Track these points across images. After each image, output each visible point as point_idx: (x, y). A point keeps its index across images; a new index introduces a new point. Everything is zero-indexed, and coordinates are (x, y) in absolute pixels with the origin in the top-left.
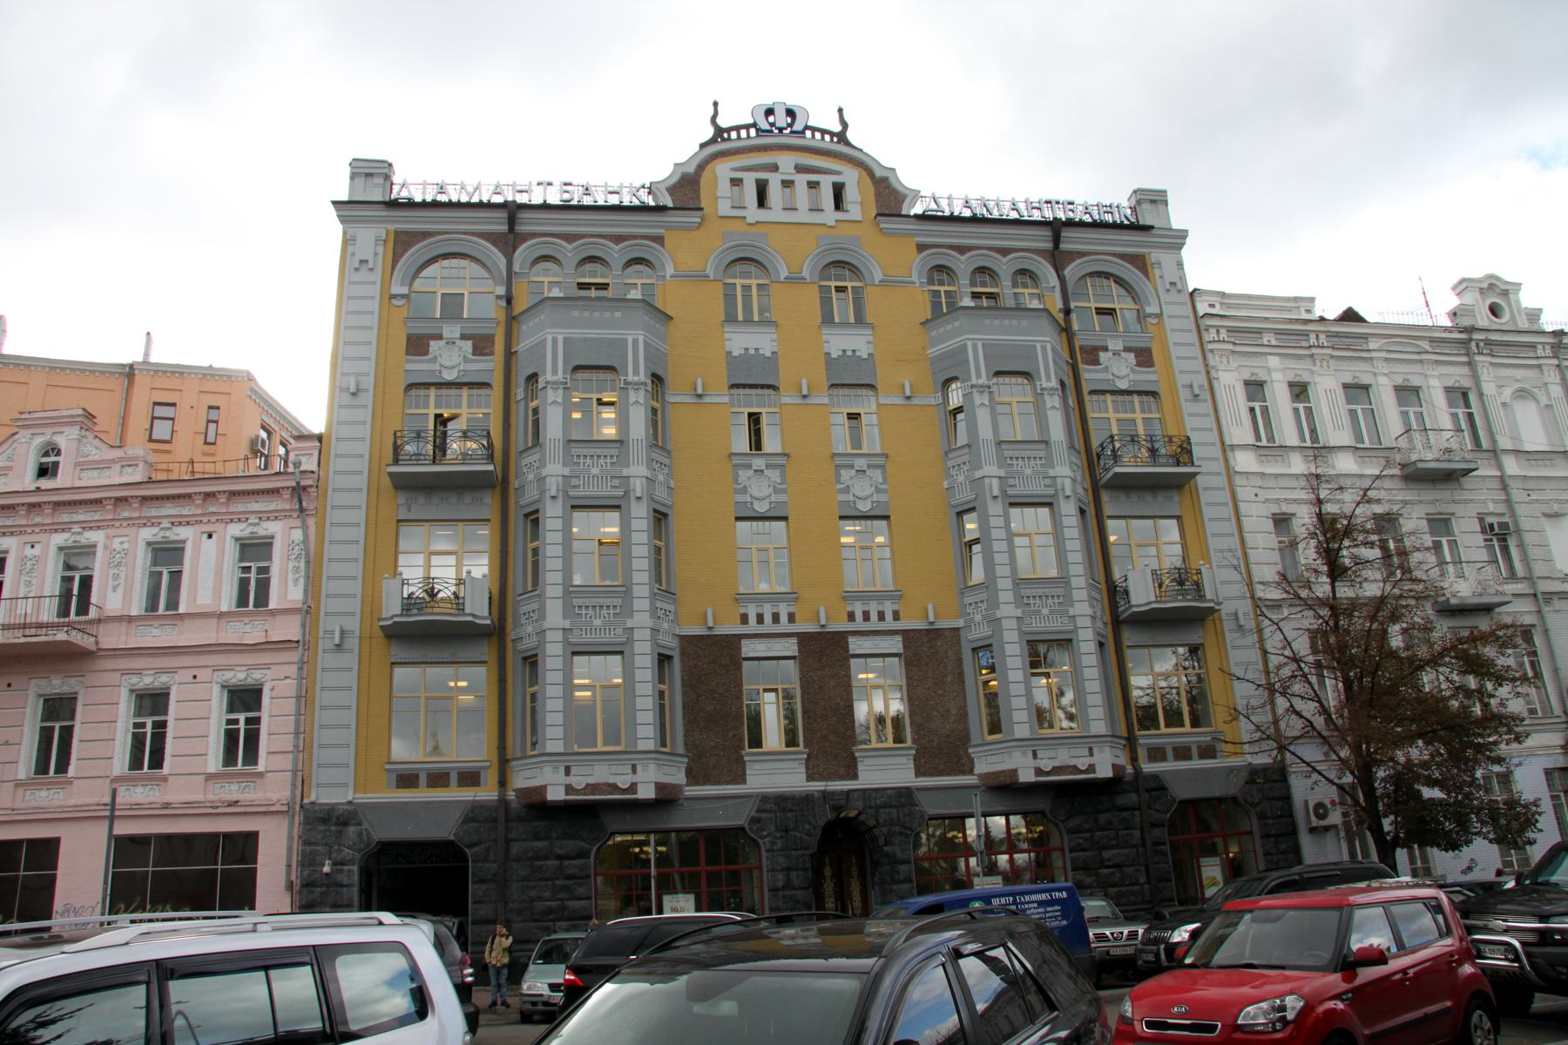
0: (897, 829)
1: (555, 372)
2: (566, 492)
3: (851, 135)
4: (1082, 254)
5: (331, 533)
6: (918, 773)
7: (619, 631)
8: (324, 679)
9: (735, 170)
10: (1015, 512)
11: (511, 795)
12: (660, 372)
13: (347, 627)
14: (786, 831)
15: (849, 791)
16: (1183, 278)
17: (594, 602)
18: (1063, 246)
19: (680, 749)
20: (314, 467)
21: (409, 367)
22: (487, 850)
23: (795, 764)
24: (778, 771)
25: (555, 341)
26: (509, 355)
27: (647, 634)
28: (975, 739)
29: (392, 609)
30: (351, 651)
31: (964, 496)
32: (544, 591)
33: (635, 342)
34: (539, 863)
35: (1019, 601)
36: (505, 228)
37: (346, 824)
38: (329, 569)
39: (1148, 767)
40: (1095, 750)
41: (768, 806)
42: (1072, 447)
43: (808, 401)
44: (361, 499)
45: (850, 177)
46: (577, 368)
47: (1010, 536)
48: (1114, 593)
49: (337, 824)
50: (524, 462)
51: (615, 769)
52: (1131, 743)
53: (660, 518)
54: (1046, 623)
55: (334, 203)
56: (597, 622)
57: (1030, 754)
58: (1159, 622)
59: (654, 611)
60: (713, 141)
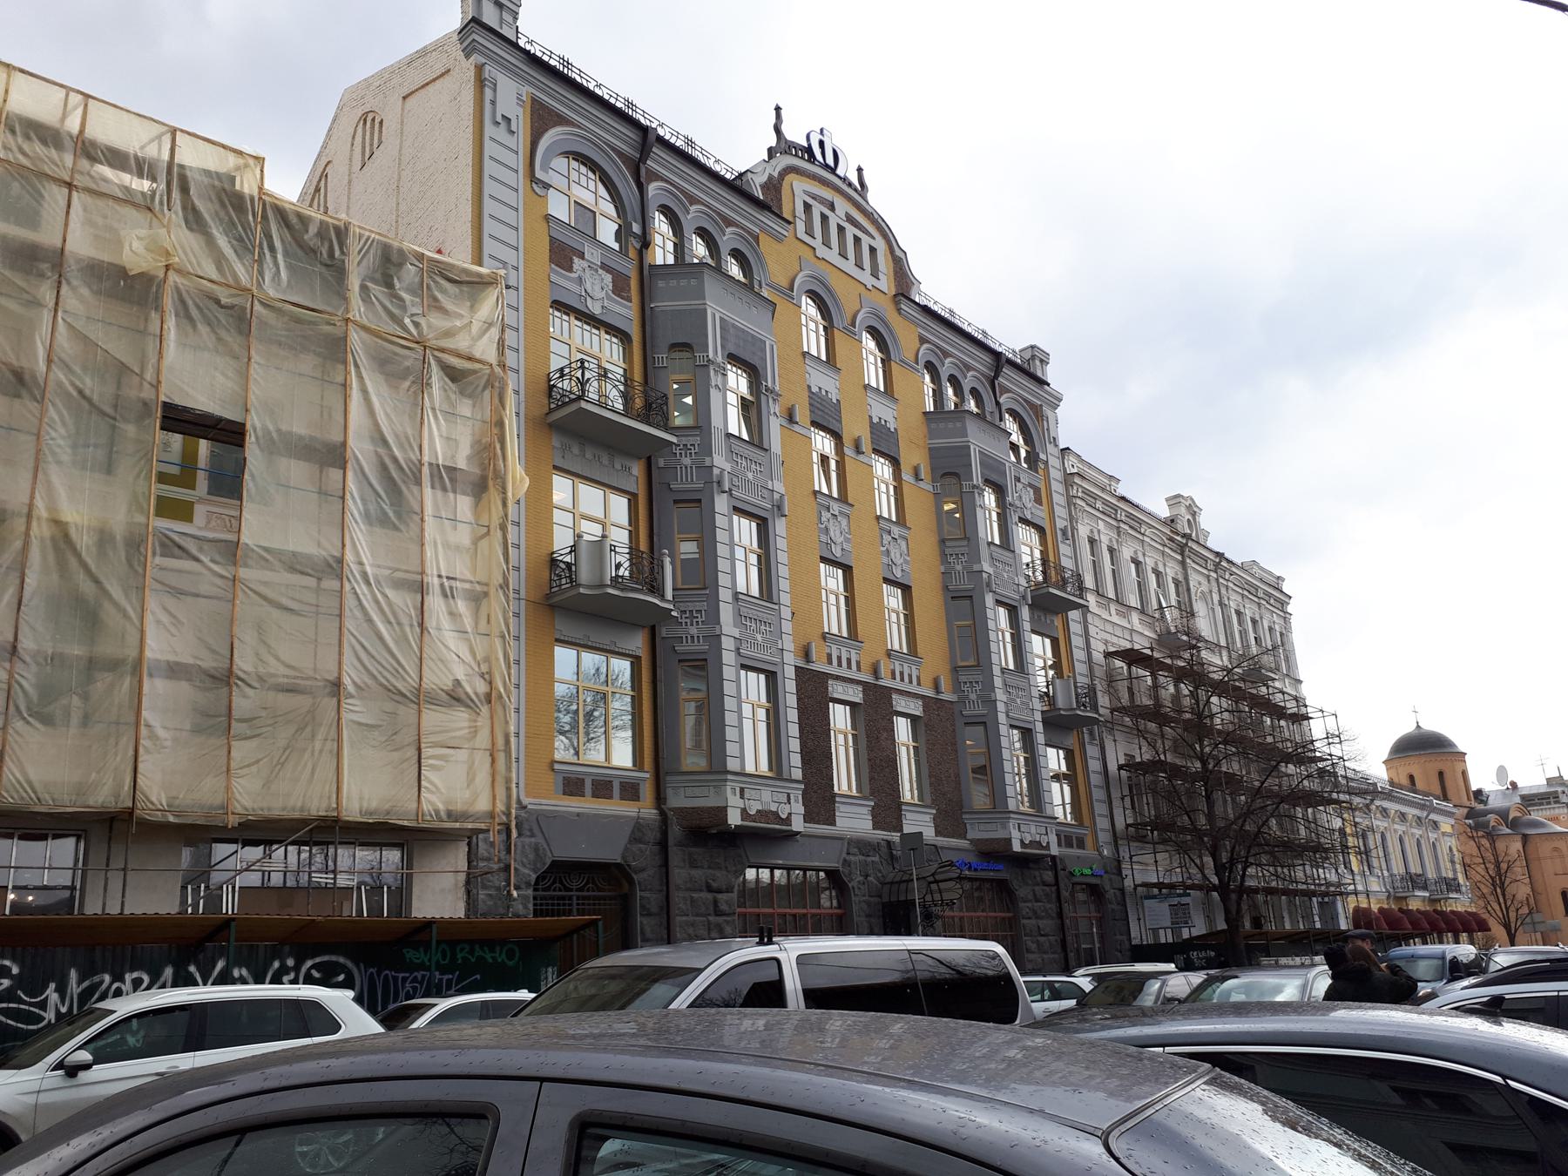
6: (938, 833)
24: (855, 821)
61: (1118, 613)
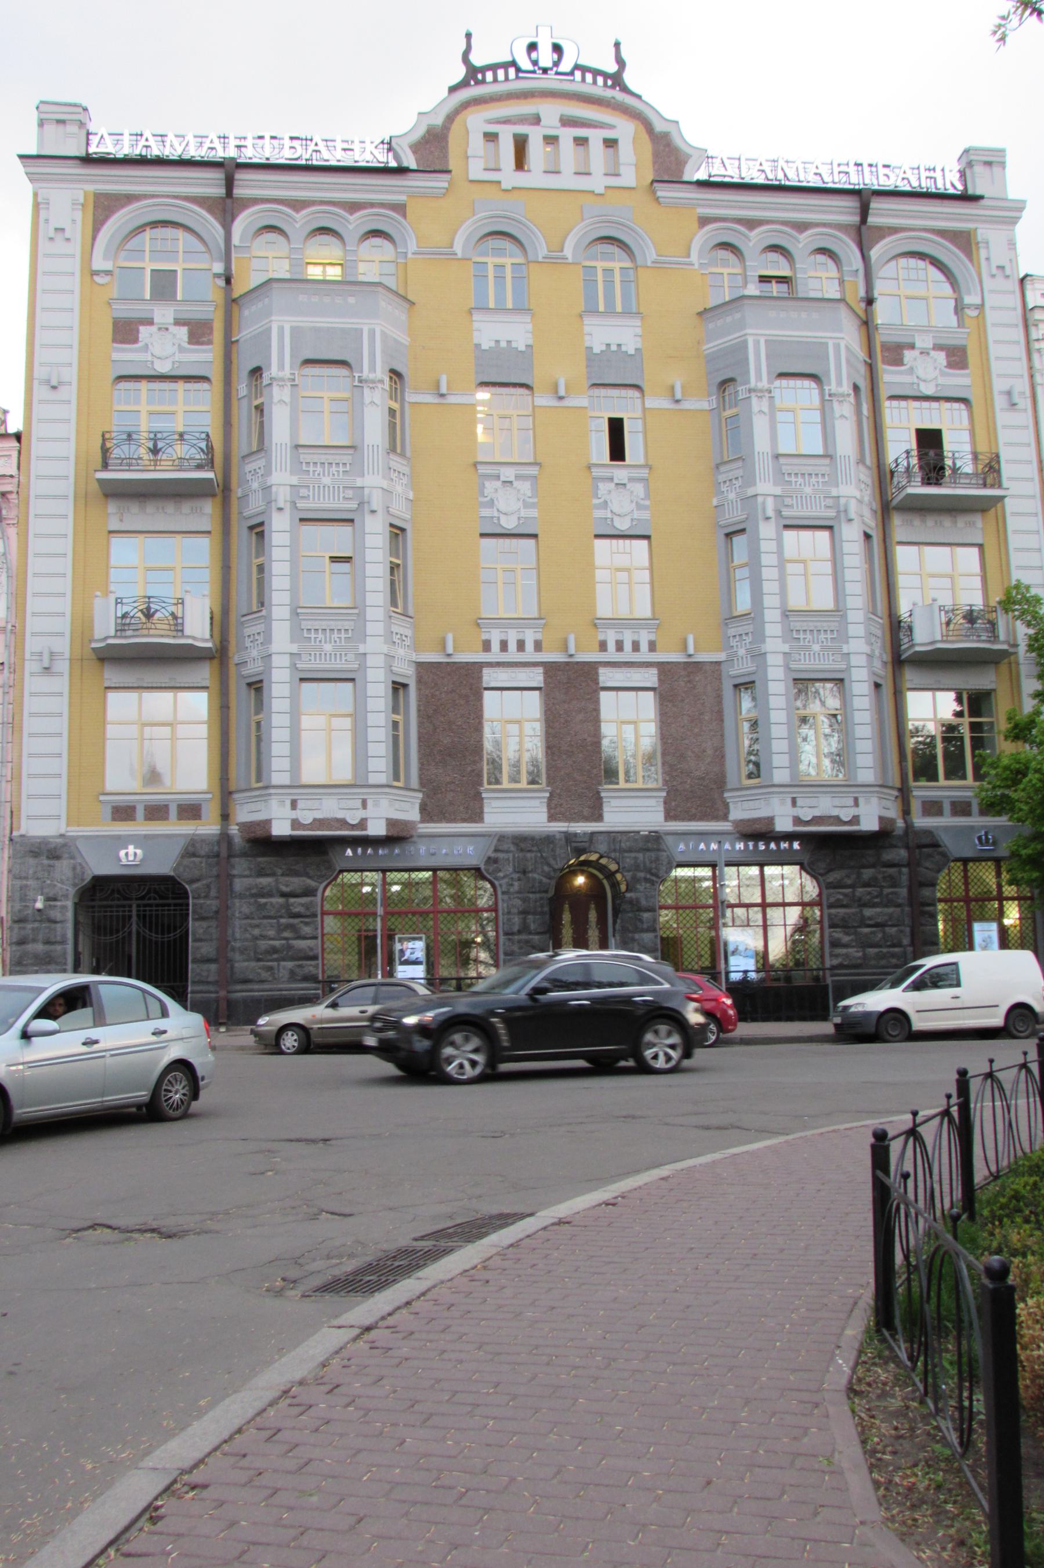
0: (642, 875)
1: (281, 367)
2: (294, 503)
3: (629, 78)
4: (894, 230)
5: (35, 545)
6: (669, 816)
7: (351, 657)
8: (31, 705)
9: (490, 122)
10: (789, 535)
11: (234, 830)
12: (399, 368)
13: (56, 649)
14: (524, 872)
15: (593, 834)
16: (1014, 261)
17: (324, 625)
18: (871, 220)
19: (415, 782)
20: (14, 471)
21: (115, 356)
22: (208, 886)
23: (536, 803)
24: (518, 811)
25: (281, 329)
26: (229, 345)
27: (380, 661)
28: (731, 780)
29: (105, 629)
30: (61, 674)
31: (734, 516)
32: (270, 612)
33: (372, 333)
34: (263, 901)
35: (789, 634)
36: (222, 191)
37: (58, 858)
38: (33, 585)
39: (920, 821)
40: (861, 801)
41: (505, 847)
42: (861, 461)
43: (566, 403)
44: (67, 507)
45: (625, 130)
46: (308, 362)
47: (782, 563)
48: (896, 628)
49: (48, 858)
50: (249, 468)
51: (344, 804)
52: (904, 794)
53: (397, 532)
54: (816, 659)
55: (21, 157)
56: (328, 647)
57: (789, 801)
58: (939, 663)
59: (389, 637)
60: (464, 84)
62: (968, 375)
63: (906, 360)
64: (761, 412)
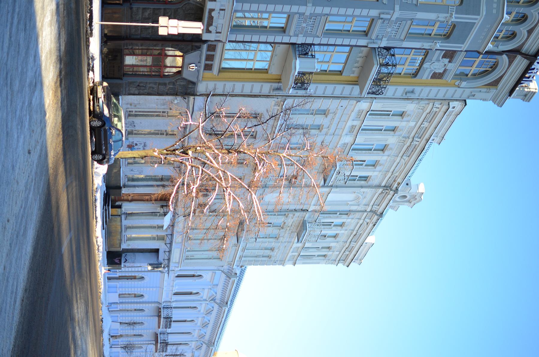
61: (353, 127)
62: (427, 78)
63: (444, 59)
64: (439, 17)
